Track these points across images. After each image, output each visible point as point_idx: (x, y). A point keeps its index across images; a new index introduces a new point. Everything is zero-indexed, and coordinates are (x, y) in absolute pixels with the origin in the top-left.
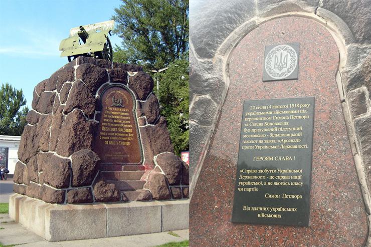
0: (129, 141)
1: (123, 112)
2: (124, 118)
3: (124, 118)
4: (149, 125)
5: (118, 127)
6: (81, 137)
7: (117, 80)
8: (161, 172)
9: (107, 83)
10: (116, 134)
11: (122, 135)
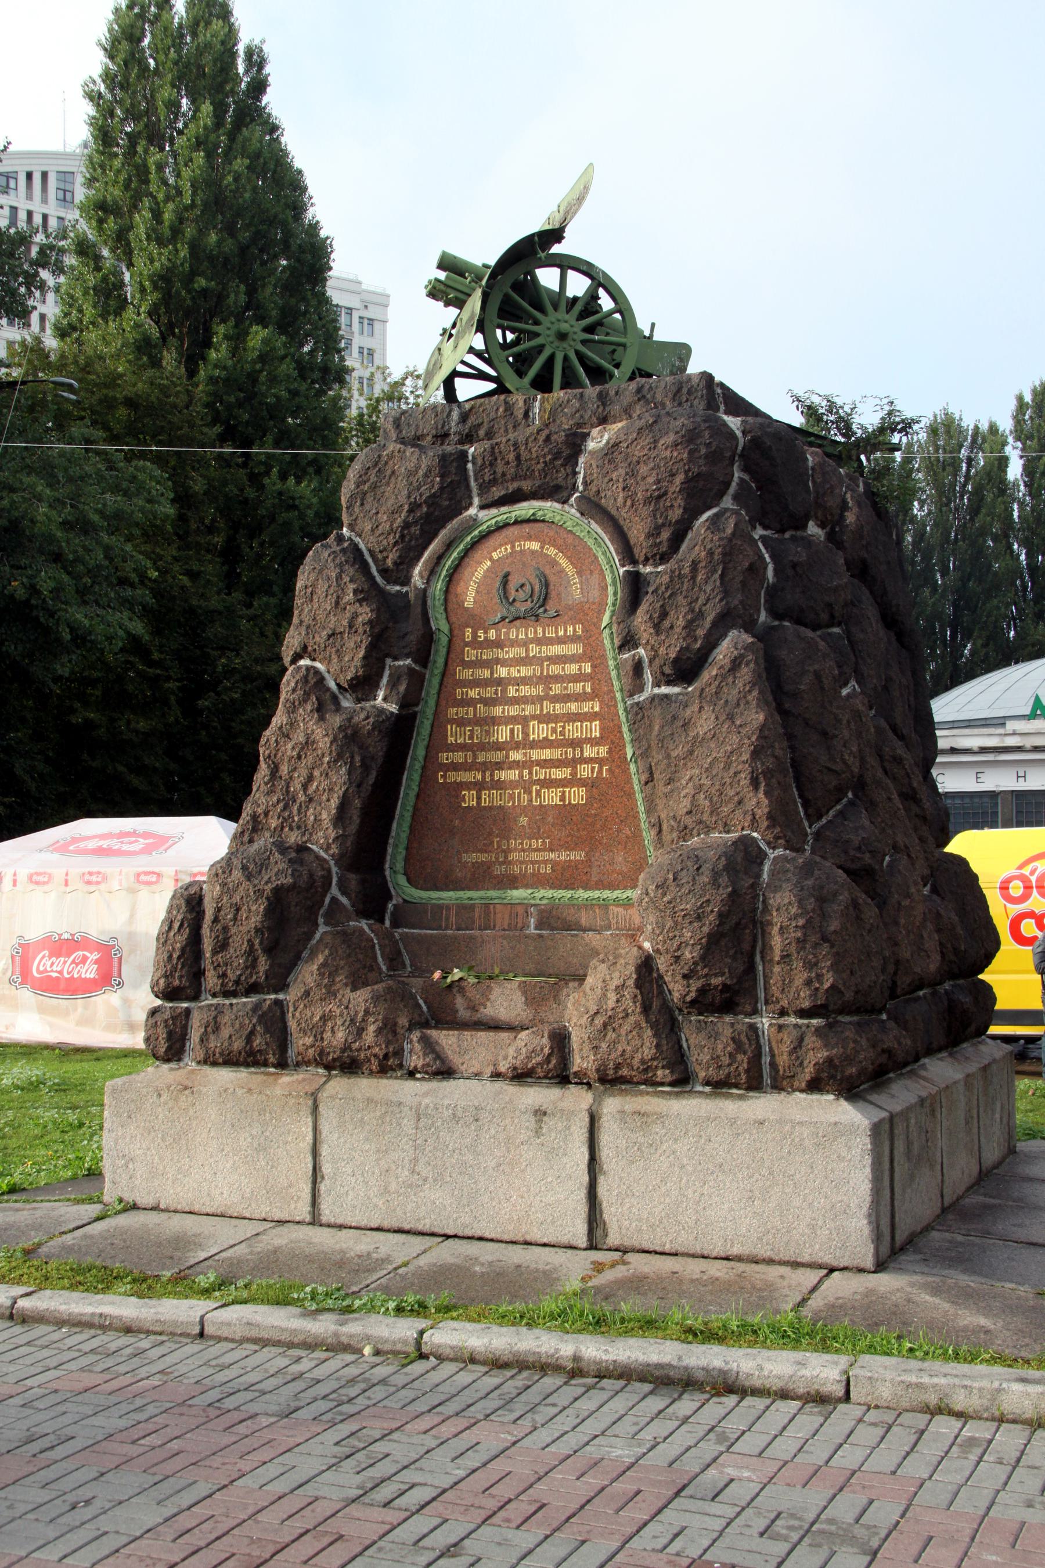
0: (582, 783)
1: (550, 642)
2: (556, 669)
3: (556, 669)
4: (664, 690)
5: (524, 721)
6: (296, 786)
7: (512, 487)
10: (515, 756)
11: (546, 754)
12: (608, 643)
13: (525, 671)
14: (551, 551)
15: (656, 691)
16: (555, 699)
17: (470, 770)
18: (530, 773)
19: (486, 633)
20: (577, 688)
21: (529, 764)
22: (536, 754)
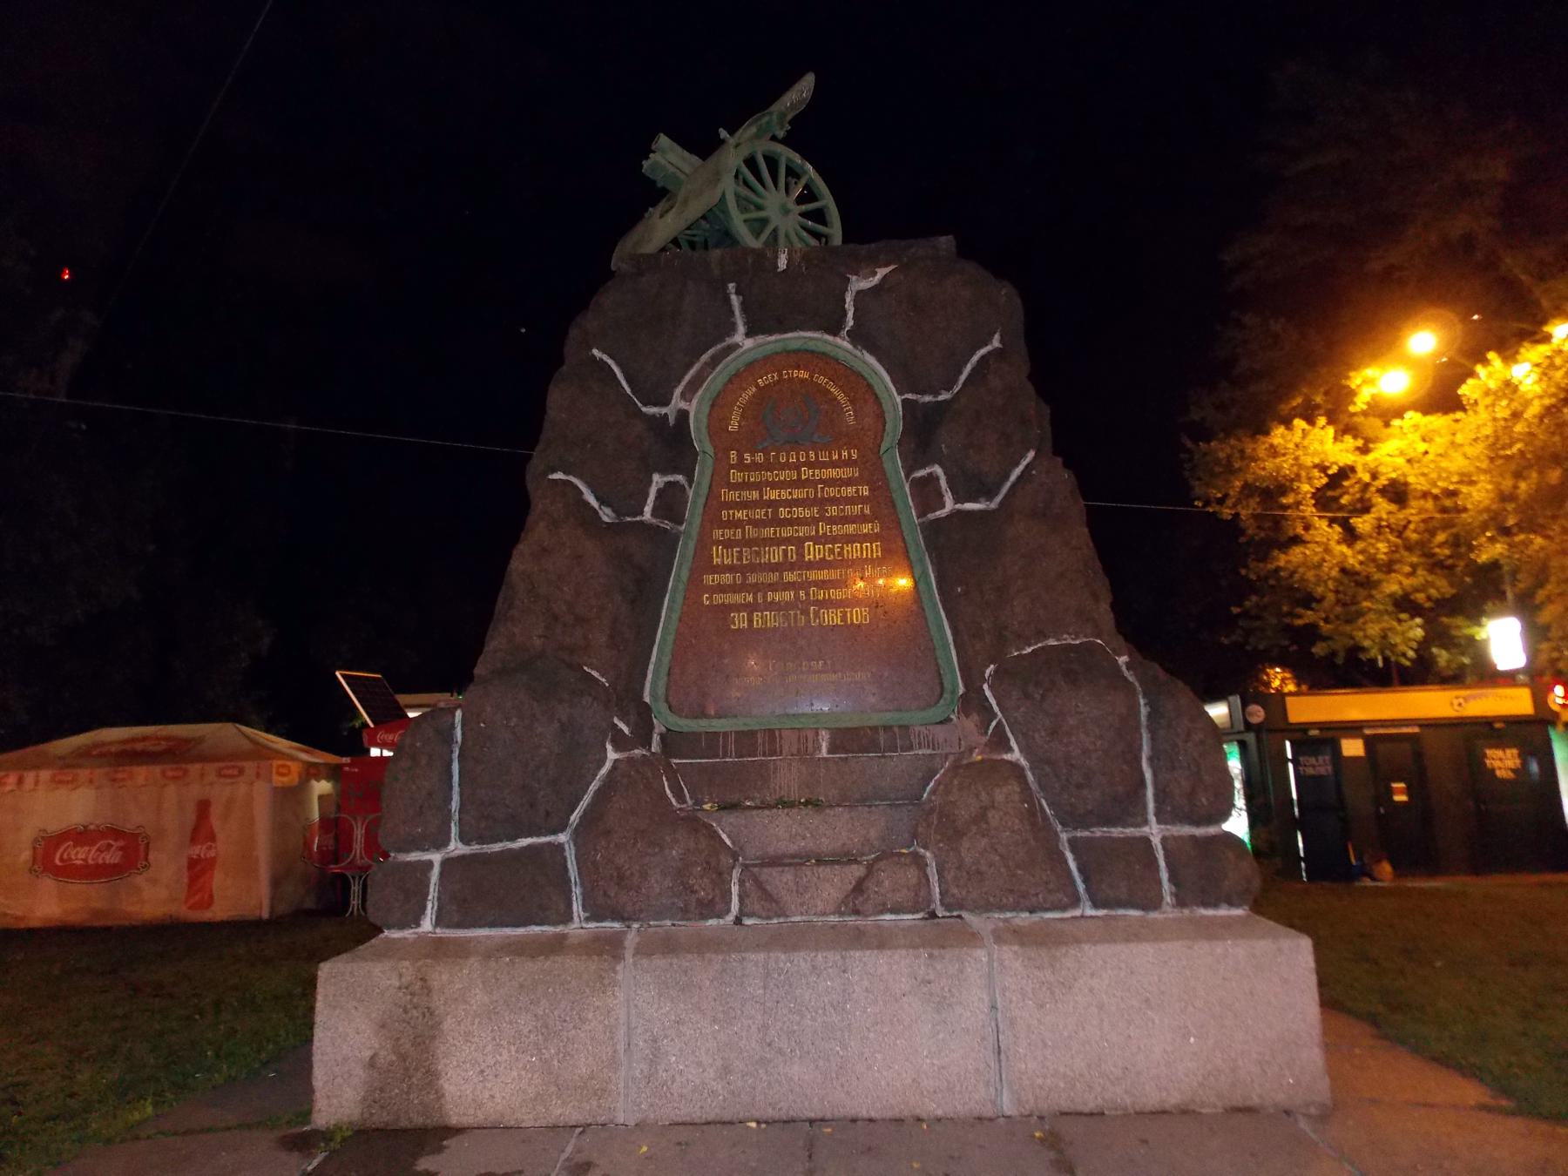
1: (824, 465)
2: (832, 492)
3: (832, 492)
5: (799, 542)
8: (1010, 750)
9: (729, 341)
10: (790, 577)
12: (894, 464)
13: (798, 494)
14: (822, 380)
15: (958, 506)
16: (832, 521)
17: (740, 591)
18: (807, 594)
19: (752, 455)
20: (857, 509)
21: (805, 585)
22: (813, 575)
